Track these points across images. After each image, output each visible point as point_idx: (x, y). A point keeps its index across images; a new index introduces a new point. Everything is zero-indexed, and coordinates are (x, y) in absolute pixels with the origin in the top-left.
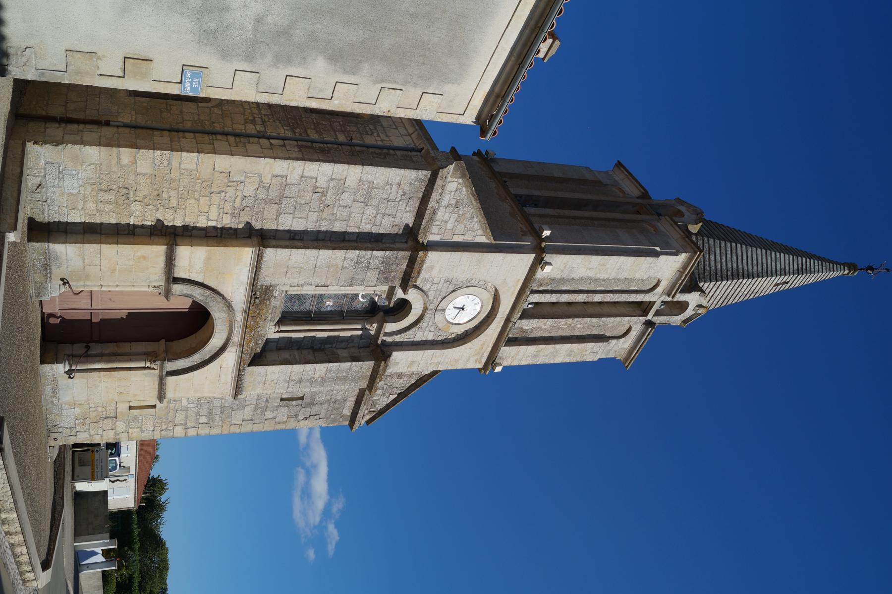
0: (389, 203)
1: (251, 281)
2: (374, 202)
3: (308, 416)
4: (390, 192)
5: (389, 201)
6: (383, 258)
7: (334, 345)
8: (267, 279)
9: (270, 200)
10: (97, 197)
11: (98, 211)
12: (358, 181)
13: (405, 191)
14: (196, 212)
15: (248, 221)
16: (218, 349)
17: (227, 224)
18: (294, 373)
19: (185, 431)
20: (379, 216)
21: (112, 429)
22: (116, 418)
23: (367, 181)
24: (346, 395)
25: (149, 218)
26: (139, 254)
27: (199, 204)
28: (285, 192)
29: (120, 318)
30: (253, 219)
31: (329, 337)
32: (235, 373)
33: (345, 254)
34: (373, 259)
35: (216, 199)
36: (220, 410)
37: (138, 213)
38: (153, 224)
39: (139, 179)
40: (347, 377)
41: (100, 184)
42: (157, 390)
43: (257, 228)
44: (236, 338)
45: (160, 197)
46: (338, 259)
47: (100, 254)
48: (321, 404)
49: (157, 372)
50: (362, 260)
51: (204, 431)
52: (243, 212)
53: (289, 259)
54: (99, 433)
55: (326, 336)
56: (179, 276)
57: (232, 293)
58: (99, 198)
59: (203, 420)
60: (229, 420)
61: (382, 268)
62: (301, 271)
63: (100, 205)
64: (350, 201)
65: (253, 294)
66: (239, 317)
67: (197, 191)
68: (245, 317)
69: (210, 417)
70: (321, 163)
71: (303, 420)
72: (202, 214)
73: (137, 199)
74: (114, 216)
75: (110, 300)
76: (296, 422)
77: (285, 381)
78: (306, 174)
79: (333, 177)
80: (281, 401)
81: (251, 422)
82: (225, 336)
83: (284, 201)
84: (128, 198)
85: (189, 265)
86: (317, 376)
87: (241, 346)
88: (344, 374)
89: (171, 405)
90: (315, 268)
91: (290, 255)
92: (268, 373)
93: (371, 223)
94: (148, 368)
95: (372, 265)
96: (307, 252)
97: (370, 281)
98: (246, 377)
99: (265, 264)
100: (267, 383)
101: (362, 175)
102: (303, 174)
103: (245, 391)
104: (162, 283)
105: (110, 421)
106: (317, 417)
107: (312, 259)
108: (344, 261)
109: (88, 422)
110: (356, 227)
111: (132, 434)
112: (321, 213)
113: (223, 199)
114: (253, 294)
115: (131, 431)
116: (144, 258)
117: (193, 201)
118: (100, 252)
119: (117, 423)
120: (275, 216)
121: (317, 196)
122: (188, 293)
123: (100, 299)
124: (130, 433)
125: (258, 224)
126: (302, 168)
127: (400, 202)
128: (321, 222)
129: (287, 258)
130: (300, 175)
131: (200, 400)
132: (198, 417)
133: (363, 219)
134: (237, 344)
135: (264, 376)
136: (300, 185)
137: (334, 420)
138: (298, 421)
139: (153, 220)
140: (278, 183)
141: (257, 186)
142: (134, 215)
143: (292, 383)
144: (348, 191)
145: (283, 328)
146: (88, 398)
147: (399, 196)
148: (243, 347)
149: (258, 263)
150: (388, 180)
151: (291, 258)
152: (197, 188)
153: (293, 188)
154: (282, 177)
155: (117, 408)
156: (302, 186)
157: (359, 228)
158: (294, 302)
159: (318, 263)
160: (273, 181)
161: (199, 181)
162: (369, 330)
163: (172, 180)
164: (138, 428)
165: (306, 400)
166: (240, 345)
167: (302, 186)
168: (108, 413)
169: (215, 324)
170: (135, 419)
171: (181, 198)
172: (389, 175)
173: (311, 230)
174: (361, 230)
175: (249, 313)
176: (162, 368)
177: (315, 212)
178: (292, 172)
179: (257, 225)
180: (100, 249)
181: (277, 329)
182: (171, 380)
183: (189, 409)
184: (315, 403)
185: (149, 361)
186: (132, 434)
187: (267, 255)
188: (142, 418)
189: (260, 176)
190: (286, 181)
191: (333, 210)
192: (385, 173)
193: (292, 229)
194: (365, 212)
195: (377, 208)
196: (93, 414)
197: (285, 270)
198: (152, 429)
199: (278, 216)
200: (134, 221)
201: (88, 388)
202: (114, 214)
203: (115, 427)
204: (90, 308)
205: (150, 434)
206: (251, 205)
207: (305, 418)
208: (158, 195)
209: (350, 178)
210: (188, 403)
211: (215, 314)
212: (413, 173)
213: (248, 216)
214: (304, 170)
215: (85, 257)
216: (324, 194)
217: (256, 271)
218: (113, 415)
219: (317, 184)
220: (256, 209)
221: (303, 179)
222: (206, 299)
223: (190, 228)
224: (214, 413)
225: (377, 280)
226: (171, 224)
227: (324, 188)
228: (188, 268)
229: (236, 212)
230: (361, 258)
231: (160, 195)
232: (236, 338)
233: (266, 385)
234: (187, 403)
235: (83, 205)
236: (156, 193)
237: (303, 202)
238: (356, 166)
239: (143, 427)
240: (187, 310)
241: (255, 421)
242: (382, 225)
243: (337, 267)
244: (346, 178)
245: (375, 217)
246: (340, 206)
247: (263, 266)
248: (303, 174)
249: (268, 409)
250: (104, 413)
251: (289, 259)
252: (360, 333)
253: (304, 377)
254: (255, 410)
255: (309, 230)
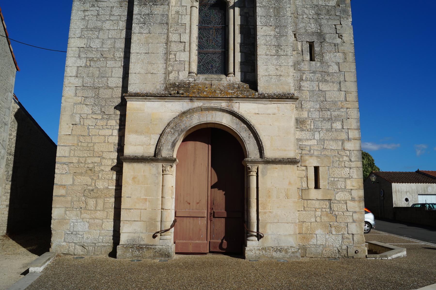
0: (100, 13)
1: (159, 99)
2: (99, 24)
3: (337, 35)
4: (91, 16)
5: (98, 15)
6: (140, 6)
7: (251, 27)
8: (158, 87)
9: (95, 95)
10: (91, 210)
11: (103, 210)
12: (81, 39)
13: (90, 6)
14: (105, 144)
15: (113, 108)
16: (234, 118)
17: (116, 122)
18: (268, 53)
19: (352, 140)
20: (112, 18)
21: (346, 203)
22: (330, 200)
23: (81, 33)
24: (308, 6)
25: (110, 176)
26: (130, 182)
27: (98, 143)
28: (89, 85)
29: (224, 196)
30: (112, 105)
31: (241, 32)
32: (264, 101)
33: (136, 33)
34: (141, 12)
35: (93, 132)
36: (324, 112)
37: (105, 183)
38: (115, 173)
39: (78, 183)
40: (275, 8)
41: (81, 208)
42: (284, 166)
43: (120, 101)
44: (224, 104)
45: (92, 169)
46: (140, 38)
47: (131, 209)
48: (320, 26)
49: (261, 166)
50: (142, 20)
51: (353, 123)
52: (106, 112)
53: (139, 73)
54: (351, 215)
55: (240, 35)
56: (153, 153)
57: (171, 112)
58: (92, 209)
59: (338, 125)
60: (339, 103)
61: (151, 4)
62: (151, 63)
63: (98, 208)
64: (97, 41)
65: (170, 96)
66: (197, 104)
67: (88, 145)
68: (197, 100)
69: (334, 119)
70: (66, 66)
71: (342, 39)
72: (106, 140)
73: (93, 184)
74: (108, 199)
75: (198, 203)
76: (344, 44)
77: (277, 59)
78: (74, 74)
79: (77, 56)
80: (314, 61)
81: (342, 83)
82: (220, 113)
83: (97, 85)
84: (92, 190)
85: (142, 146)
86: (272, 33)
87: (230, 99)
88: (271, 10)
89: (316, 153)
90: (148, 53)
91: (135, 73)
92: (267, 74)
93: (118, 23)
94: (257, 173)
95: (147, 12)
96: (133, 61)
97: (164, 10)
98: (271, 92)
99: (143, 90)
100: (279, 73)
101: (76, 37)
102: (74, 76)
103: (290, 90)
104: (160, 165)
105: (335, 207)
106: (338, 27)
107: (139, 56)
108: (143, 33)
109: (336, 223)
110: (121, 32)
111: (353, 186)
112: (108, 59)
113: (94, 127)
114: (170, 96)
115: (349, 187)
116: (134, 178)
117: (95, 147)
118: (128, 209)
119: (337, 199)
120: (110, 90)
121: (93, 64)
122: (170, 145)
123: (197, 211)
124: (353, 188)
125: (116, 101)
126: (70, 77)
127: (100, 6)
128: (116, 57)
129: (139, 75)
130: (75, 78)
131: (310, 129)
132: (333, 130)
133: (114, 28)
134: (230, 103)
135: (270, 77)
136: (83, 77)
137: (344, 11)
138: (344, 42)
139: (112, 173)
140: (81, 92)
141: (84, 105)
142: (107, 186)
143: (281, 53)
144: (89, 44)
145: (231, 70)
146: (292, 223)
147: (94, 9)
148: (230, 98)
149: (138, 95)
150: (80, 19)
151: (138, 72)
152: (85, 145)
153: (86, 81)
154: (76, 90)
155: (317, 199)
156: (85, 75)
157: (123, 30)
158: (212, 66)
159: (143, 52)
160: (80, 95)
161: (80, 144)
162: (234, 3)
163: (79, 162)
164: (345, 182)
165: (314, 39)
166: (229, 100)
167: (85, 75)
168: (325, 207)
169: (206, 122)
170: (333, 183)
171: (93, 155)
172: (76, 19)
173: (123, 63)
174: (125, 28)
175: (192, 97)
176: (254, 162)
177: (106, 63)
178: (72, 84)
179: (118, 101)
180: (126, 209)
181: (233, 75)
182: (269, 154)
183: (322, 138)
184: (319, 31)
185: (250, 173)
186: (353, 186)
187: (134, 90)
188: (332, 177)
189: (75, 104)
190: (80, 87)
191: (106, 51)
192: (75, 23)
193: (122, 76)
194: (108, 28)
195: (104, 21)
196: (325, 219)
197: (149, 75)
198: (348, 169)
199: (110, 88)
200: (113, 186)
201: (278, 223)
202: (106, 199)
203: (343, 201)
204: (206, 219)
205: (355, 171)
206: (99, 107)
207: (340, 36)
208: (91, 170)
209: (78, 45)
210: (314, 139)
211: (194, 123)
212: (75, 4)
213: (109, 108)
214: (71, 76)
215: (133, 220)
216: (92, 60)
217: (147, 96)
218: (327, 203)
219: (84, 65)
220: (103, 103)
221: (79, 75)
222: (178, 131)
223: (120, 148)
224: (329, 117)
225: (163, 5)
226: (116, 161)
227: (87, 60)
228: (145, 146)
229: (106, 117)
230: (140, 21)
231: (90, 169)
232: (224, 104)
233: (282, 74)
234: (313, 141)
235: (99, 219)
236: (90, 172)
237: (98, 72)
238: (68, 42)
239: (344, 176)
240: (210, 146)
241: (342, 79)
242: (119, 14)
243: (148, 37)
244: (78, 47)
245: (112, 21)
246: (102, 47)
247: (145, 92)
248: (74, 76)
249: (326, 70)
250: (324, 210)
251: (139, 73)
252: (237, 10)
253: (273, 43)
254: (326, 81)
255: (123, 65)
